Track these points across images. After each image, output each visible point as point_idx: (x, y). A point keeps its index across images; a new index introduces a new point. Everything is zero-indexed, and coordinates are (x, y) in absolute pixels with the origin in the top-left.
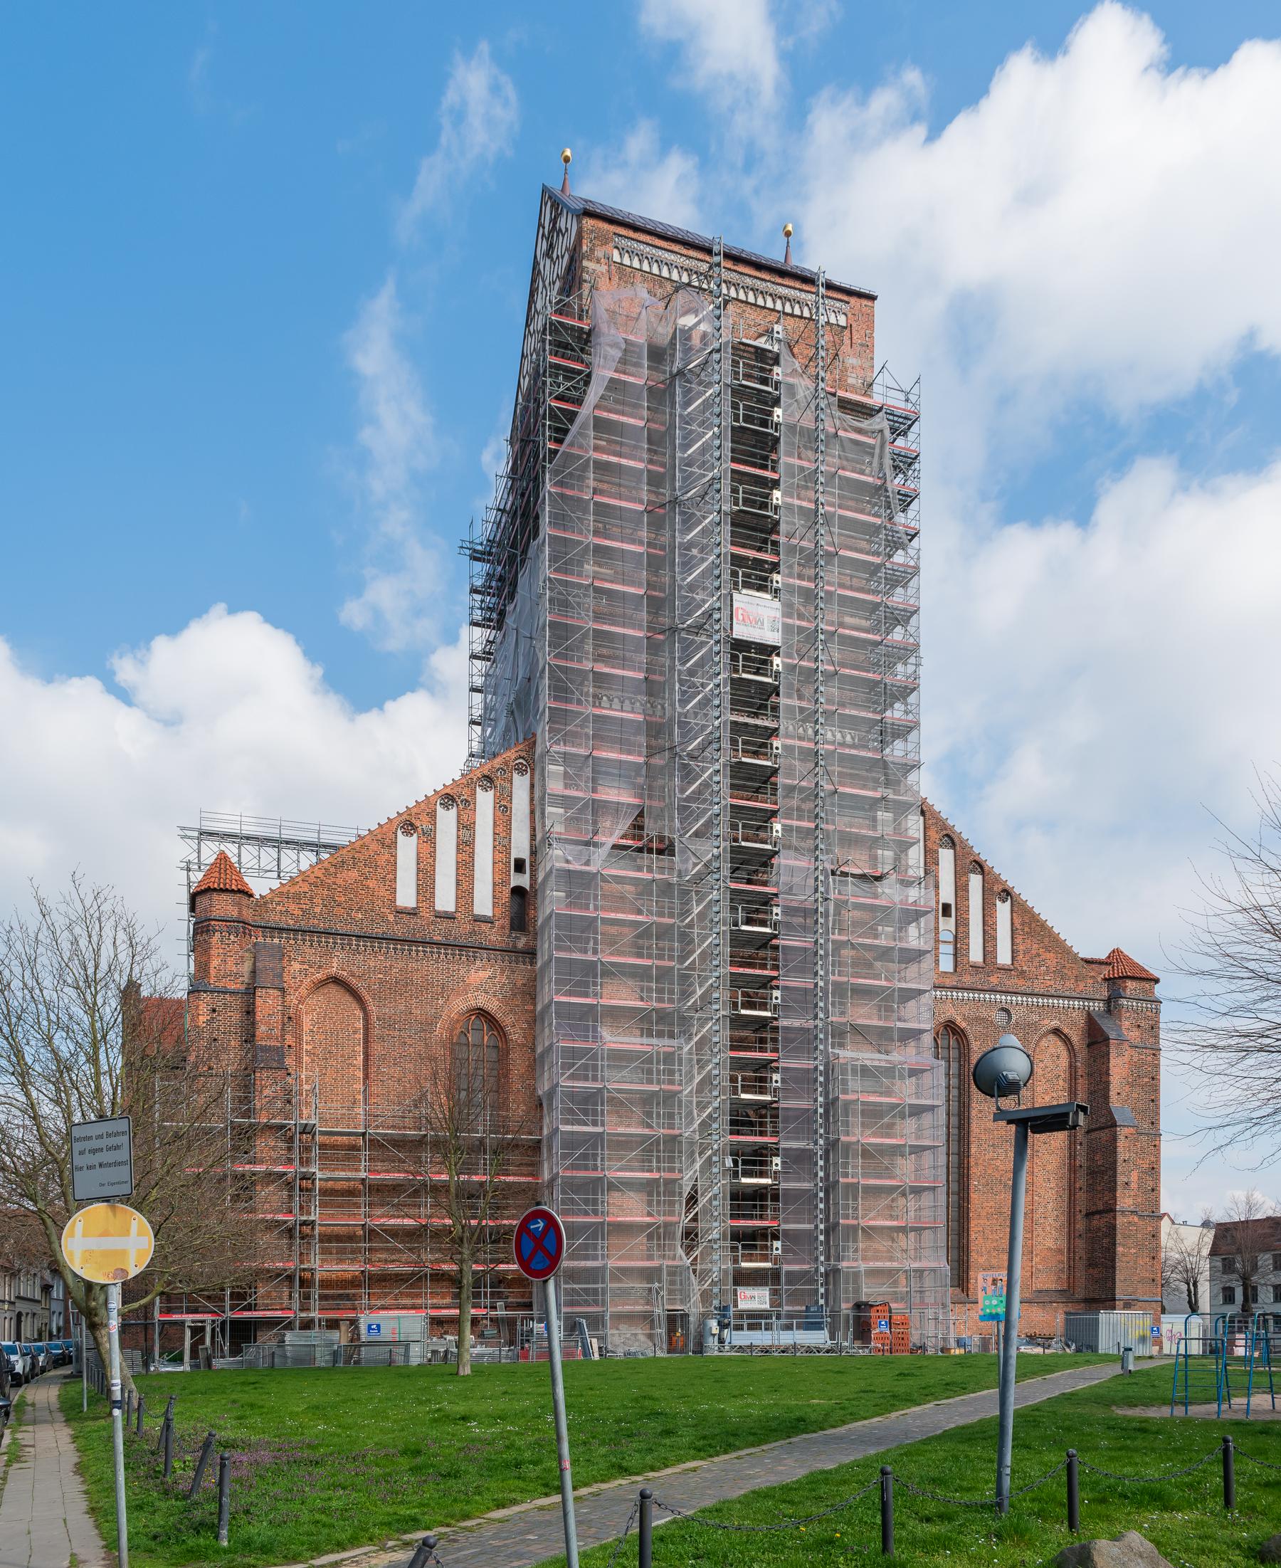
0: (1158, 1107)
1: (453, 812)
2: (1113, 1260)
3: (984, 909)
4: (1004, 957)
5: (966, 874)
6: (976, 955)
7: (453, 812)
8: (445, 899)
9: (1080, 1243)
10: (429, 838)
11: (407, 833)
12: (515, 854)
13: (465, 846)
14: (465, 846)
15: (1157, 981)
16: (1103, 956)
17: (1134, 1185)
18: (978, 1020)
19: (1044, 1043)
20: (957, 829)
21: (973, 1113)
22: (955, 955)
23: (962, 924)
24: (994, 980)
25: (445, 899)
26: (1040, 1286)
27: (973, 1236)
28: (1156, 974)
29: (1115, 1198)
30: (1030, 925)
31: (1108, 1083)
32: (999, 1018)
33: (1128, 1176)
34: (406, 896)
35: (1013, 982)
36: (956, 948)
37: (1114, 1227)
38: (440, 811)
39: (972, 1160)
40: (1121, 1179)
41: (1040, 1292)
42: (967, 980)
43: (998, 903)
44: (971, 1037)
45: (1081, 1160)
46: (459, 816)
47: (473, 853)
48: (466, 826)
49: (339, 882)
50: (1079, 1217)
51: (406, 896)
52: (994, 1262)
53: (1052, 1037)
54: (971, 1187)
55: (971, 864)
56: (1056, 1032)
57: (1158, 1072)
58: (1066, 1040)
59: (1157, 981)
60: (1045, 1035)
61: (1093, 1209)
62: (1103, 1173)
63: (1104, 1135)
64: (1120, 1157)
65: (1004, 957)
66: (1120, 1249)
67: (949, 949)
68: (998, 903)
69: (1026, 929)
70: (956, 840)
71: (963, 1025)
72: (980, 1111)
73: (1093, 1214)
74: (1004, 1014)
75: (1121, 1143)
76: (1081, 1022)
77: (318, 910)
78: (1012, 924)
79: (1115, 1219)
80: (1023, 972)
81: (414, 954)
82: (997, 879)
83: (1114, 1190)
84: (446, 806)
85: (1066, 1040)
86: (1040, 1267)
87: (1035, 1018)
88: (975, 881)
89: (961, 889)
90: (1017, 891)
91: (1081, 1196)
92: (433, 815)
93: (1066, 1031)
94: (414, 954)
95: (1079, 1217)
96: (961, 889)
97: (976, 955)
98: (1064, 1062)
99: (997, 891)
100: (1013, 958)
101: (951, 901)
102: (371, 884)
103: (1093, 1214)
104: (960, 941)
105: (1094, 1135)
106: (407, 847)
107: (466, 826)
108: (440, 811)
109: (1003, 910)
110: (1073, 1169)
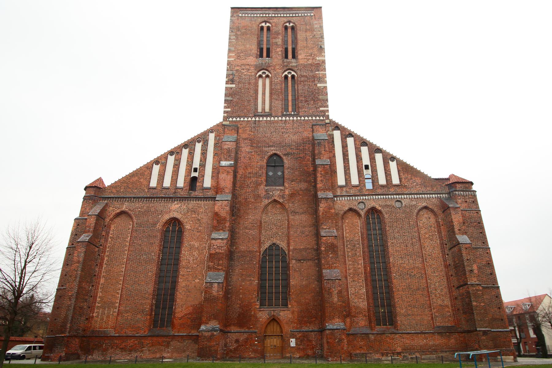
6: (382, 180)
12: (194, 166)
21: (389, 244)
24: (392, 190)
36: (372, 180)
42: (379, 191)
43: (390, 162)
44: (384, 213)
52: (410, 312)
55: (374, 150)
71: (380, 208)
72: (393, 243)
74: (399, 203)
86: (437, 314)
89: (372, 159)
96: (372, 159)
97: (382, 180)
99: (388, 158)
104: (374, 178)
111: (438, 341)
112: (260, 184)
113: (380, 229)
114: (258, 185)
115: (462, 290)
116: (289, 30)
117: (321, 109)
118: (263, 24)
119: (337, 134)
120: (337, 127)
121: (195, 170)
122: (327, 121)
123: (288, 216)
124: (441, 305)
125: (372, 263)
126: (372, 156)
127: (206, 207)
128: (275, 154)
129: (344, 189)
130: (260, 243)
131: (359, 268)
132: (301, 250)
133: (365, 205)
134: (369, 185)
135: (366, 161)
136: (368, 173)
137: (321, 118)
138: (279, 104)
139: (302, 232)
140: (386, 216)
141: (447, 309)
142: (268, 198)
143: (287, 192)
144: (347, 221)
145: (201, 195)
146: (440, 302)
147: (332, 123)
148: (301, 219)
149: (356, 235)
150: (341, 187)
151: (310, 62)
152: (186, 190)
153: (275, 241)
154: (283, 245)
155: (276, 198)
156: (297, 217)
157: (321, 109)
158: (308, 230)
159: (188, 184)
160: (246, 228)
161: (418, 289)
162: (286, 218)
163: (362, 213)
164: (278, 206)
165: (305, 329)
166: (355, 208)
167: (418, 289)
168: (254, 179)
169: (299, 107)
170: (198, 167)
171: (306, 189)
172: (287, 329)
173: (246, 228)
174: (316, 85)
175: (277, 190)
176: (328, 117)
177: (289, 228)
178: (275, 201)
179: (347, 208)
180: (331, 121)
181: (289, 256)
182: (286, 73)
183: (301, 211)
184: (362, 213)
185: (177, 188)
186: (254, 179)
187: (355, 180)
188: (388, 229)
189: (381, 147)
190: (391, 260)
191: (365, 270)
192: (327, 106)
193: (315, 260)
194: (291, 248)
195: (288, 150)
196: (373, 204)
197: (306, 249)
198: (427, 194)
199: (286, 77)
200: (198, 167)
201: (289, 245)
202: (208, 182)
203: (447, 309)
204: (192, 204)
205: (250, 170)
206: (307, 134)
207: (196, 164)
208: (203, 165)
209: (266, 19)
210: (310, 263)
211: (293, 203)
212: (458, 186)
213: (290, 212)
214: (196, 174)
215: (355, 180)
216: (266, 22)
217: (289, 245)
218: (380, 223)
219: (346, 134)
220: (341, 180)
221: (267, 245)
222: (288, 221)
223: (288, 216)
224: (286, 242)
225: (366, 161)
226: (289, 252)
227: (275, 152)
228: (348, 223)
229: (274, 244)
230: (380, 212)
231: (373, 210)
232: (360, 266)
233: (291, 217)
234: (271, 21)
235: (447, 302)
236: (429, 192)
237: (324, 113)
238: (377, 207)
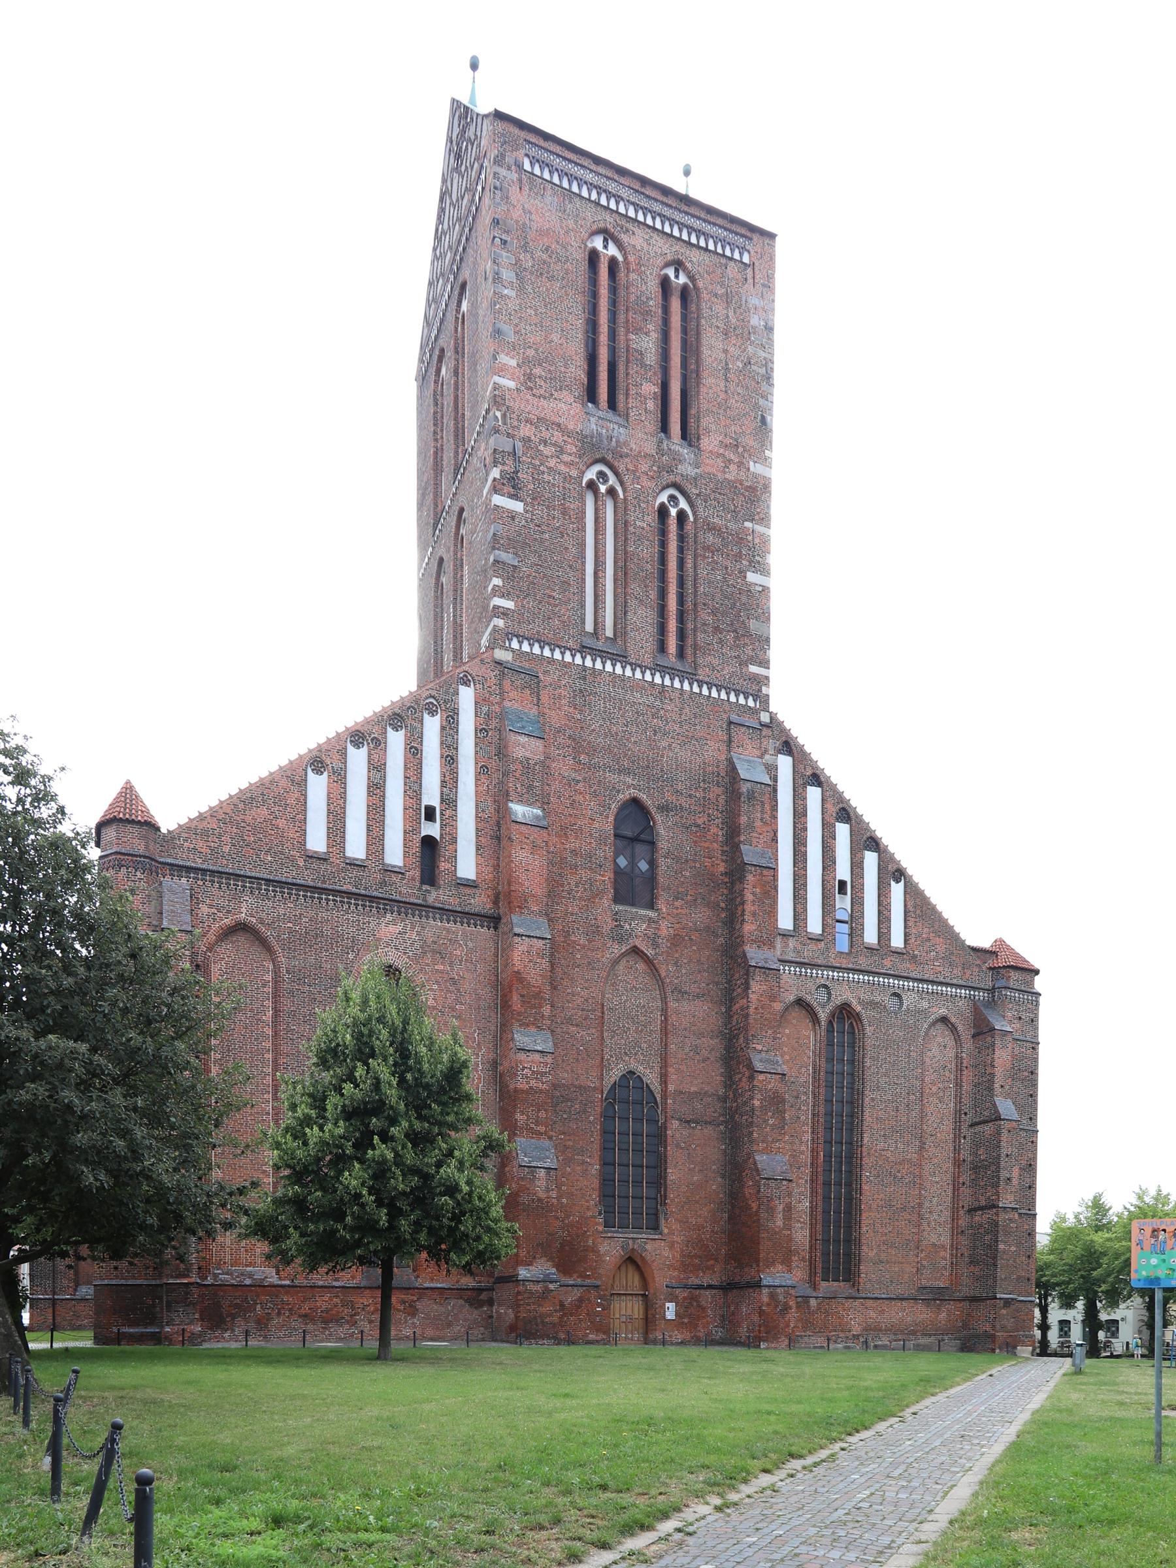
0: (1036, 1102)
1: (363, 752)
2: (995, 1258)
3: (879, 889)
4: (897, 940)
5: (861, 850)
6: (871, 936)
7: (363, 752)
8: (356, 847)
9: (964, 1241)
10: (339, 779)
11: (318, 772)
13: (376, 789)
14: (376, 789)
15: (1037, 972)
16: (986, 943)
17: (1015, 1181)
18: (873, 1004)
19: (933, 1032)
20: (853, 803)
21: (867, 1100)
22: (851, 935)
23: (858, 902)
24: (887, 962)
25: (356, 847)
26: (924, 1282)
27: (864, 1229)
28: (1037, 966)
29: (997, 1194)
30: (920, 908)
31: (992, 1075)
32: (891, 1003)
33: (1010, 1172)
34: (317, 841)
35: (904, 967)
36: (852, 928)
37: (996, 1224)
38: (351, 749)
39: (864, 1149)
40: (1004, 1174)
41: (925, 1288)
42: (863, 962)
43: (893, 883)
44: (865, 1022)
45: (965, 1154)
46: (370, 755)
47: (384, 796)
48: (377, 768)
49: (249, 819)
50: (962, 1212)
51: (317, 841)
52: (883, 1256)
53: (940, 1026)
54: (864, 1178)
56: (944, 1020)
57: (1036, 1066)
58: (954, 1029)
59: (1037, 972)
60: (934, 1024)
61: (976, 1204)
62: (986, 1168)
63: (988, 1129)
64: (1004, 1152)
65: (897, 941)
66: (1001, 1246)
67: (845, 928)
68: (893, 883)
69: (918, 912)
70: (852, 814)
71: (858, 1008)
73: (975, 1210)
74: (896, 1000)
75: (1005, 1136)
76: (968, 1013)
77: (226, 849)
78: (905, 906)
79: (997, 1215)
80: (914, 957)
81: (324, 902)
82: (891, 858)
83: (996, 1185)
84: (357, 745)
85: (954, 1029)
86: (924, 1263)
87: (925, 1004)
88: (871, 860)
89: (857, 866)
90: (910, 872)
91: (966, 1191)
92: (343, 754)
93: (953, 1020)
94: (324, 902)
95: (962, 1212)
96: (857, 866)
97: (871, 936)
98: (951, 1053)
99: (892, 872)
100: (906, 941)
101: (847, 877)
102: (281, 823)
103: (975, 1210)
104: (855, 920)
105: (978, 1128)
106: (318, 786)
107: (377, 768)
108: (351, 749)
109: (897, 890)
110: (958, 1163)
111: (920, 1314)
112: (599, 894)
113: (852, 1061)
114: (594, 897)
115: (978, 1217)
116: (675, 304)
117: (753, 669)
118: (598, 243)
119: (785, 764)
120: (788, 746)
121: (430, 814)
122: (765, 718)
123: (664, 1000)
124: (934, 1245)
125: (828, 1142)
126: (859, 855)
127: (470, 945)
128: (635, 801)
129: (792, 943)
130: (602, 1066)
131: (802, 1153)
132: (692, 1096)
133: (829, 994)
134: (843, 943)
135: (843, 871)
136: (843, 903)
137: (751, 703)
138: (642, 618)
139: (696, 1049)
140: (869, 1030)
141: (942, 1254)
142: (620, 940)
143: (665, 929)
144: (787, 1031)
145: (453, 903)
146: (933, 1238)
147: (774, 725)
148: (696, 1014)
149: (804, 1070)
150: (785, 935)
151: (732, 474)
152: (413, 879)
153: (633, 1066)
154: (651, 1078)
155: (638, 943)
156: (685, 1006)
157: (753, 669)
158: (712, 1046)
159: (415, 860)
160: (569, 1021)
161: (904, 1209)
162: (659, 1004)
163: (823, 1016)
164: (641, 966)
165: (694, 1280)
166: (808, 998)
167: (904, 1209)
168: (584, 874)
169: (696, 647)
170: (435, 802)
171: (708, 929)
172: (661, 1279)
173: (569, 1021)
174: (743, 573)
175: (642, 918)
176: (765, 701)
177: (665, 1031)
178: (635, 950)
179: (792, 998)
180: (773, 717)
181: (664, 1110)
182: (663, 498)
183: (694, 989)
184: (823, 1016)
185: (388, 870)
186: (584, 874)
187: (814, 925)
188: (868, 1064)
189: (879, 834)
190: (866, 1140)
191: (814, 1158)
192: (765, 664)
193: (719, 1125)
194: (671, 1088)
195: (669, 797)
196: (842, 995)
197: (700, 1095)
198: (952, 985)
199: (663, 512)
200: (435, 802)
201: (664, 1079)
202: (467, 865)
203: (942, 1254)
204: (435, 927)
205: (572, 843)
206: (713, 751)
207: (431, 796)
208: (449, 801)
209: (609, 221)
210: (709, 1131)
211: (676, 963)
212: (1014, 975)
213: (669, 990)
214: (432, 830)
215: (814, 925)
216: (608, 235)
217: (664, 1079)
218: (852, 1045)
219: (810, 776)
220: (785, 921)
221: (615, 1074)
222: (665, 1011)
223: (664, 1000)
224: (657, 1069)
225: (843, 871)
226: (664, 1093)
227: (633, 792)
228: (788, 1036)
229: (631, 1073)
230: (857, 1017)
231: (844, 1012)
232: (803, 1148)
233: (672, 1004)
234: (624, 238)
235: (946, 1240)
236: (955, 981)
237: (757, 688)
238: (854, 1003)
